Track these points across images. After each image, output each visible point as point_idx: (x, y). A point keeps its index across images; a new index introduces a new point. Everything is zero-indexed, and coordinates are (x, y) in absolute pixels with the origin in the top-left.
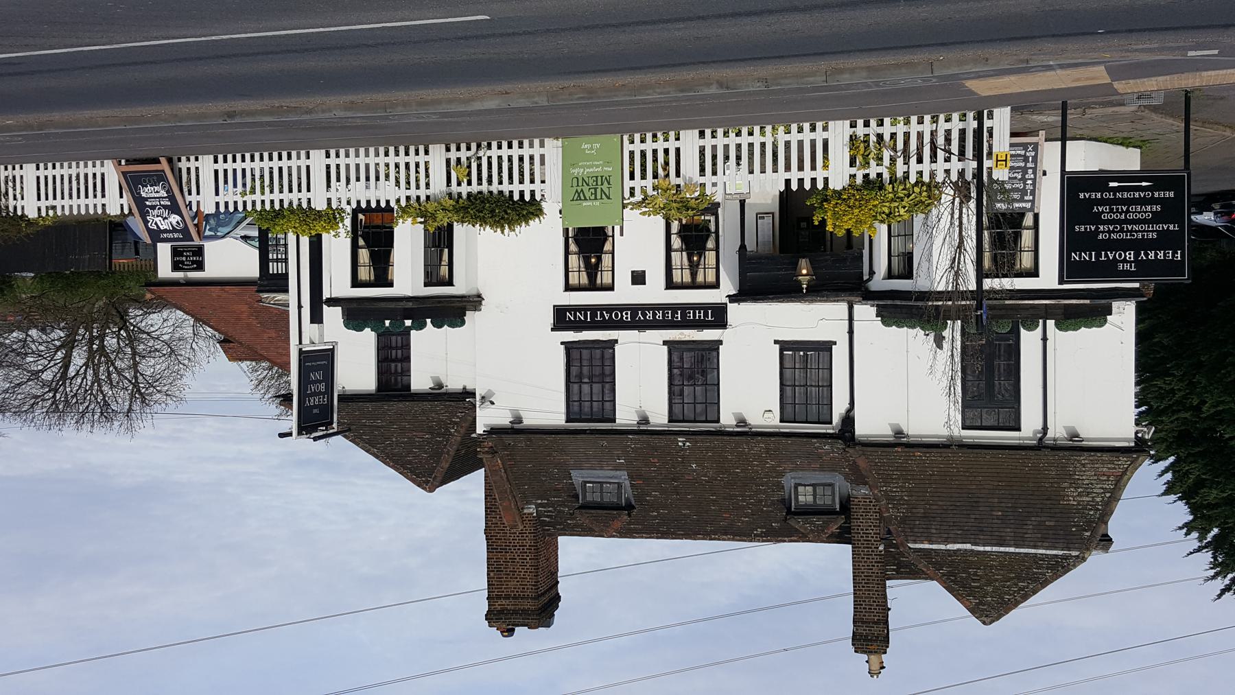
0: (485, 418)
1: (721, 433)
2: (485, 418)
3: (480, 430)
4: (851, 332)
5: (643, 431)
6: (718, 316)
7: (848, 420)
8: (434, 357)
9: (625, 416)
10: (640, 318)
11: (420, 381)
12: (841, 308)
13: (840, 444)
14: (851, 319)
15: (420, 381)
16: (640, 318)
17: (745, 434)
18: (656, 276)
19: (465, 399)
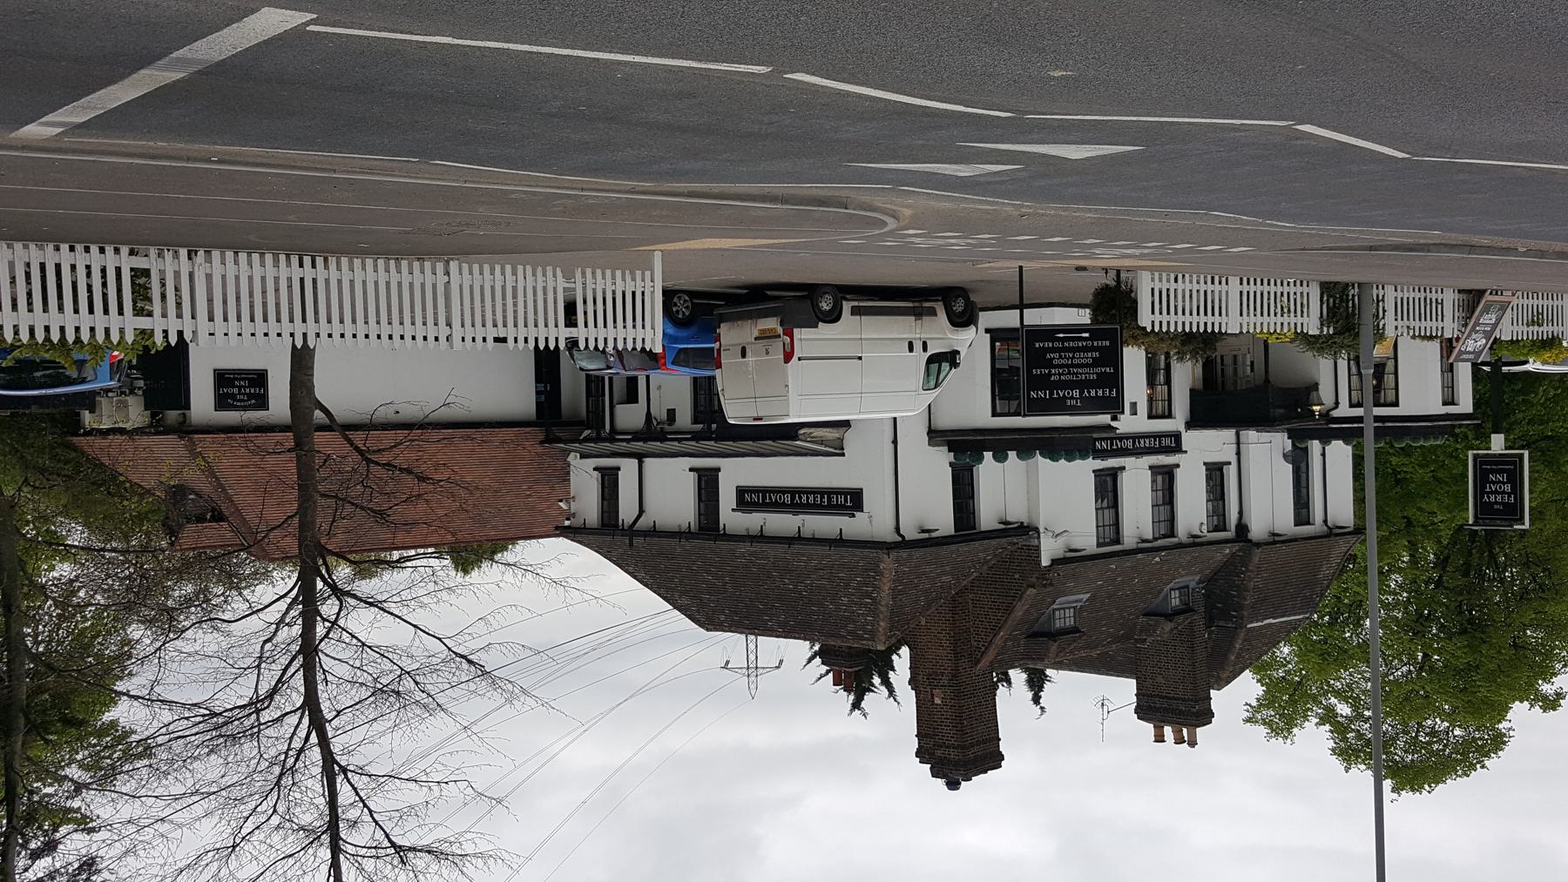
0: (1049, 549)
1: (1181, 546)
2: (1049, 549)
3: (1045, 562)
4: (1238, 453)
5: (1145, 548)
6: (1173, 444)
7: (1242, 528)
8: (1003, 487)
9: (1130, 537)
10: (1137, 445)
11: (988, 515)
12: (1228, 434)
13: (1236, 547)
14: (1238, 443)
15: (988, 515)
16: (1137, 445)
17: (1195, 542)
18: (1143, 408)
19: (1027, 530)
